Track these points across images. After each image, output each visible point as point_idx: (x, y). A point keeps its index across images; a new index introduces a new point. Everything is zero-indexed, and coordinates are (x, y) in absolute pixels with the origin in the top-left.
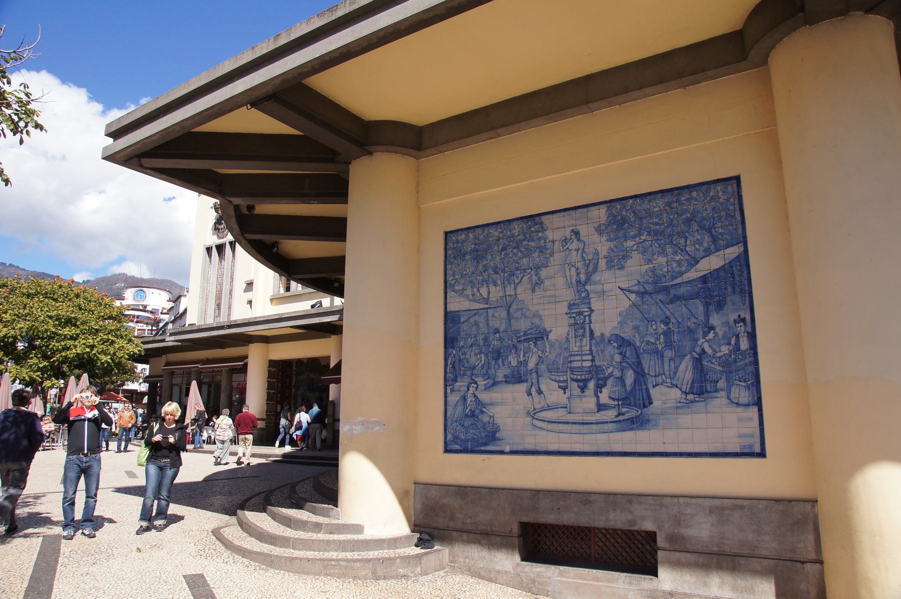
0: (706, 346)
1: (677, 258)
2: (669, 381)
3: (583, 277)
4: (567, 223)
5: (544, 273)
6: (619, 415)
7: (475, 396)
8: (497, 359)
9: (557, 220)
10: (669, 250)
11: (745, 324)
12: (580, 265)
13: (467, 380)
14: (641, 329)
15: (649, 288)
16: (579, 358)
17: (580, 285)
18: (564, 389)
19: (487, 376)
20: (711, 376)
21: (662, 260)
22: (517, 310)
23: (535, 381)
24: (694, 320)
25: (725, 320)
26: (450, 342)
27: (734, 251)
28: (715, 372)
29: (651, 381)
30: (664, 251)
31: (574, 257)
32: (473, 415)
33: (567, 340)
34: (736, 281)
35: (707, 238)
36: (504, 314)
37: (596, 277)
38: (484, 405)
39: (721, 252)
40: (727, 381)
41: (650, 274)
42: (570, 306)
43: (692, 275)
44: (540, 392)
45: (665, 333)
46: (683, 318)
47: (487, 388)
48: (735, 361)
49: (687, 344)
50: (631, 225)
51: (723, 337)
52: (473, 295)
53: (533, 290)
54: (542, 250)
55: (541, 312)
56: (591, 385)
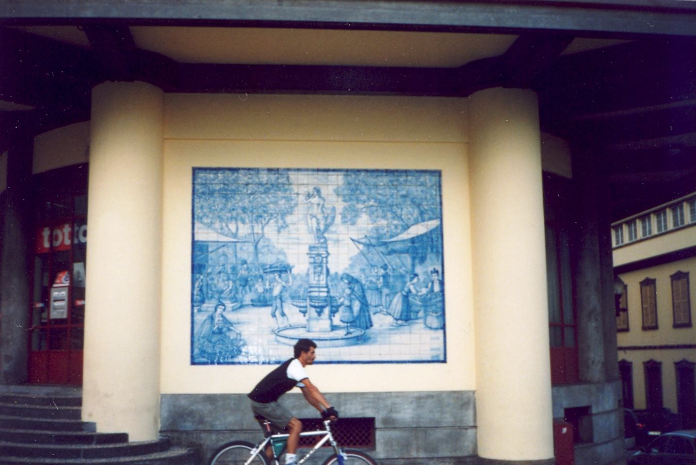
0: (412, 287)
1: (395, 222)
2: (385, 310)
3: (322, 227)
4: (310, 182)
5: (289, 219)
6: (348, 333)
7: (222, 316)
8: (244, 286)
9: (303, 178)
10: (389, 215)
11: (438, 274)
12: (320, 216)
13: (214, 302)
14: (367, 271)
15: (373, 241)
16: (316, 289)
17: (320, 234)
18: (304, 313)
19: (234, 299)
20: (414, 308)
21: (384, 222)
22: (264, 246)
23: (279, 305)
24: (404, 268)
25: (425, 270)
26: (197, 268)
27: (434, 224)
28: (417, 306)
29: (372, 310)
30: (386, 216)
31: (316, 210)
32: (220, 332)
33: (308, 275)
34: (431, 246)
35: (416, 212)
36: (252, 249)
37: (332, 228)
38: (231, 324)
39: (425, 223)
40: (425, 311)
41: (375, 231)
42: (311, 248)
43: (405, 236)
44: (283, 315)
45: (384, 276)
46: (397, 266)
47: (234, 310)
48: (430, 299)
49: (399, 285)
50: (362, 193)
51: (424, 282)
52: (222, 229)
53: (279, 231)
54: (288, 199)
55: (286, 251)
56: (327, 311)
